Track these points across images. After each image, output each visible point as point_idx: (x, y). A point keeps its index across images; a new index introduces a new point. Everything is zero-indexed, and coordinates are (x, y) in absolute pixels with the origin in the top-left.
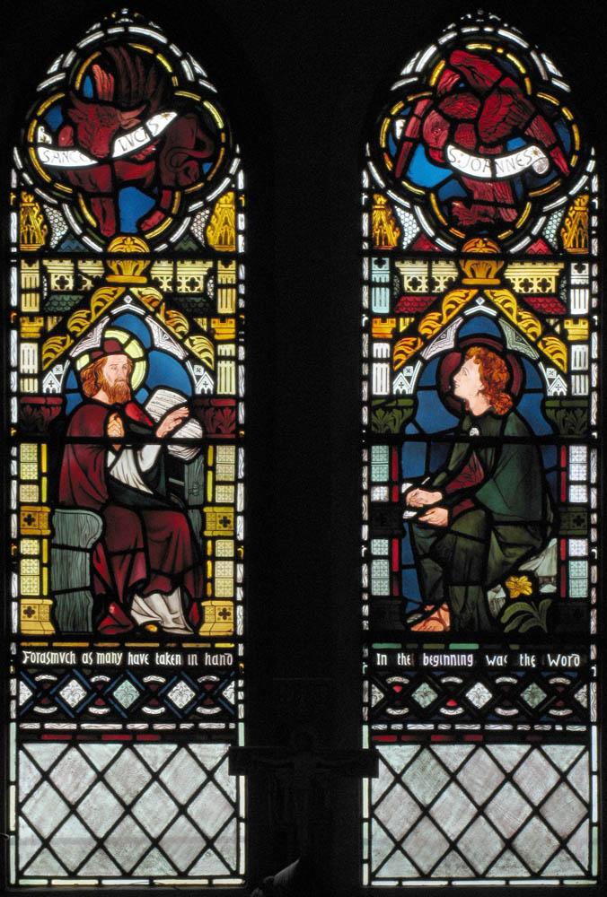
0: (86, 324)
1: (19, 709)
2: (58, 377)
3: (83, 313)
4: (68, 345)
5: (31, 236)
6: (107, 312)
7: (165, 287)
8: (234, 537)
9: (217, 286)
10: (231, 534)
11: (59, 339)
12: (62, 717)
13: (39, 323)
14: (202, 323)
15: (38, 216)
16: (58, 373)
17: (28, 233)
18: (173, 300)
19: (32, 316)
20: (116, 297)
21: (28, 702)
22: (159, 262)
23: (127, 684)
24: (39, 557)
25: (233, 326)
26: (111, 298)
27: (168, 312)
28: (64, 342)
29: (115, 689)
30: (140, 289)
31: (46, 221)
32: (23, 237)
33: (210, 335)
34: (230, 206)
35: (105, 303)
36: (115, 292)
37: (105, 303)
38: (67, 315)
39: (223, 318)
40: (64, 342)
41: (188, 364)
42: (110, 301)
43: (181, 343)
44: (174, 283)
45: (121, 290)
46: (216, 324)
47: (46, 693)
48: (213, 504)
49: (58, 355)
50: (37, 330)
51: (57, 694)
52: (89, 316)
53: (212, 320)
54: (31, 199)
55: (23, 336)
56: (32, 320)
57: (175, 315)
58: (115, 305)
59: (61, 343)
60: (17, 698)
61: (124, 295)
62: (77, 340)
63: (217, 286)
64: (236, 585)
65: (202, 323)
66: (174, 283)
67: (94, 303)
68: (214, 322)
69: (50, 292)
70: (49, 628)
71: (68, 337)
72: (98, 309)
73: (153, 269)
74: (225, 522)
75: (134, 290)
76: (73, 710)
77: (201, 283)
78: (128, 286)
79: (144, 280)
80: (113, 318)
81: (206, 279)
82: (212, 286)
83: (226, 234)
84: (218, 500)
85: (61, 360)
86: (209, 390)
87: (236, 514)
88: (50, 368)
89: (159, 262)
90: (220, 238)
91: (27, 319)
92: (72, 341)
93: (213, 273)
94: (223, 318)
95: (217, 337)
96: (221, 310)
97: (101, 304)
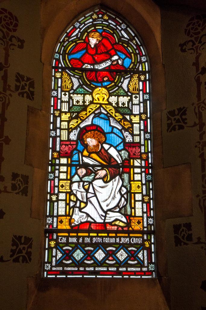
1: (56, 261)
2: (75, 134)
3: (84, 113)
5: (66, 86)
7: (114, 105)
8: (142, 193)
9: (132, 104)
10: (141, 191)
11: (75, 121)
12: (73, 265)
13: (68, 115)
14: (128, 117)
15: (69, 80)
16: (75, 133)
17: (65, 85)
18: (117, 109)
19: (66, 113)
20: (96, 108)
21: (60, 258)
22: (111, 97)
23: (100, 251)
24: (66, 200)
25: (139, 118)
26: (94, 108)
27: (115, 114)
28: (77, 122)
29: (95, 253)
30: (106, 106)
31: (72, 82)
32: (63, 86)
33: (130, 121)
34: (137, 79)
35: (92, 110)
36: (96, 106)
37: (92, 110)
38: (78, 113)
39: (135, 115)
40: (77, 122)
41: (123, 131)
42: (94, 109)
44: (117, 103)
45: (98, 106)
46: (132, 117)
47: (89, 255)
48: (134, 181)
49: (75, 126)
51: (93, 256)
52: (86, 114)
53: (131, 116)
54: (67, 74)
55: (62, 119)
56: (66, 114)
57: (118, 115)
58: (96, 110)
59: (76, 122)
60: (56, 257)
62: (82, 121)
63: (132, 104)
64: (143, 212)
65: (128, 117)
66: (117, 103)
67: (88, 110)
68: (132, 117)
69: (73, 105)
70: (68, 227)
71: (79, 119)
72: (90, 112)
73: (109, 99)
74: (138, 187)
75: (104, 106)
76: (78, 262)
77: (126, 103)
80: (95, 114)
81: (128, 103)
82: (131, 104)
83: (135, 87)
84: (135, 179)
85: (76, 128)
86: (131, 141)
87: (142, 184)
89: (111, 97)
90: (133, 89)
91: (64, 114)
92: (81, 121)
93: (131, 100)
94: (135, 115)
95: (133, 122)
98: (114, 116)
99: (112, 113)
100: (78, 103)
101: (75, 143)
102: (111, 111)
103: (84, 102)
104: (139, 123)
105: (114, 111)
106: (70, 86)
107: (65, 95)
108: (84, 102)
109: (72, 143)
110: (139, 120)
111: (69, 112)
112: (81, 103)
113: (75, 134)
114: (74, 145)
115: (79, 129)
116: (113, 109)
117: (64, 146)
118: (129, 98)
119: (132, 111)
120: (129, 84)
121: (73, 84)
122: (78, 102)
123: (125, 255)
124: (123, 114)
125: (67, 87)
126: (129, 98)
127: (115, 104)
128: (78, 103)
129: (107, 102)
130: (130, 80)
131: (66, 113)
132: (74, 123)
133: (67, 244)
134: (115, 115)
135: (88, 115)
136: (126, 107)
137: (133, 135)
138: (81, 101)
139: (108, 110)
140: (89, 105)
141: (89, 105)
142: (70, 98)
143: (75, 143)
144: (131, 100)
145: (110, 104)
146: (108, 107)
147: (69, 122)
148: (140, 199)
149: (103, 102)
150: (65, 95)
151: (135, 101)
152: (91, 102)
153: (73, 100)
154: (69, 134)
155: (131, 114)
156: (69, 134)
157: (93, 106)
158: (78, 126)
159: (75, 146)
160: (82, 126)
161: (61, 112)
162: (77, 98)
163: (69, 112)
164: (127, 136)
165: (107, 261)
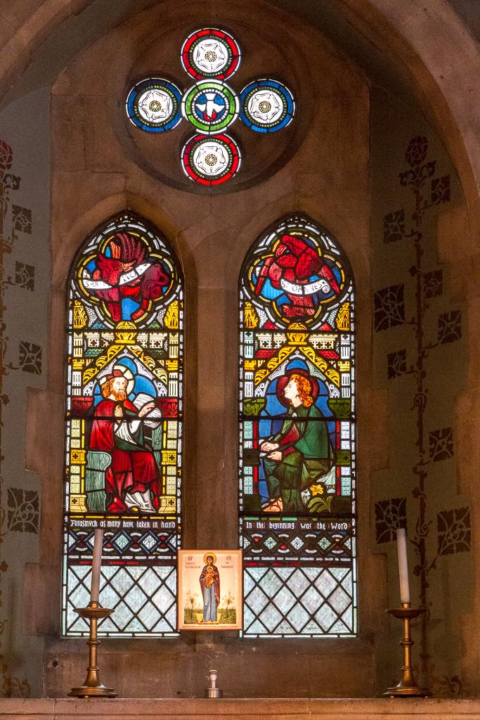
0: (276, 364)
2: (262, 389)
4: (267, 374)
6: (288, 358)
7: (315, 346)
19: (250, 360)
25: (349, 365)
28: (266, 373)
31: (257, 316)
33: (338, 369)
38: (267, 359)
39: (344, 361)
40: (266, 373)
42: (288, 353)
43: (323, 374)
46: (340, 364)
50: (253, 366)
52: (278, 361)
61: (295, 350)
62: (271, 372)
78: (297, 346)
79: (305, 343)
81: (335, 343)
85: (264, 381)
88: (258, 385)
91: (248, 361)
93: (338, 339)
94: (344, 361)
95: (341, 370)
96: (343, 358)
97: (283, 355)
98: (314, 361)
99: (311, 357)
100: (265, 346)
101: (263, 401)
102: (310, 355)
103: (274, 344)
104: (350, 372)
105: (313, 354)
106: (255, 324)
107: (249, 334)
108: (274, 344)
109: (259, 401)
110: (349, 367)
111: (254, 359)
112: (269, 346)
113: (262, 389)
114: (261, 403)
115: (268, 382)
116: (314, 352)
117: (248, 405)
118: (336, 336)
119: (339, 355)
120: (336, 316)
121: (259, 318)
122: (265, 344)
123: (301, 544)
124: (327, 360)
125: (251, 323)
126: (336, 336)
127: (317, 345)
128: (265, 346)
129: (305, 343)
130: (338, 312)
131: (250, 360)
132: (261, 373)
133: (255, 530)
134: (316, 361)
135: (280, 362)
136: (331, 350)
137: (339, 389)
138: (270, 343)
139: (306, 353)
140: (281, 348)
141: (281, 348)
142: (255, 338)
143: (263, 401)
144: (338, 339)
145: (310, 345)
146: (305, 349)
147: (254, 372)
148: (348, 473)
149: (301, 343)
150: (249, 334)
151: (344, 341)
152: (284, 345)
153: (259, 341)
154: (255, 387)
155: (338, 358)
156: (255, 387)
157: (286, 350)
158: (266, 379)
159: (263, 405)
160: (272, 377)
161: (244, 359)
162: (264, 338)
163: (254, 359)
164: (332, 390)
165: (279, 551)
